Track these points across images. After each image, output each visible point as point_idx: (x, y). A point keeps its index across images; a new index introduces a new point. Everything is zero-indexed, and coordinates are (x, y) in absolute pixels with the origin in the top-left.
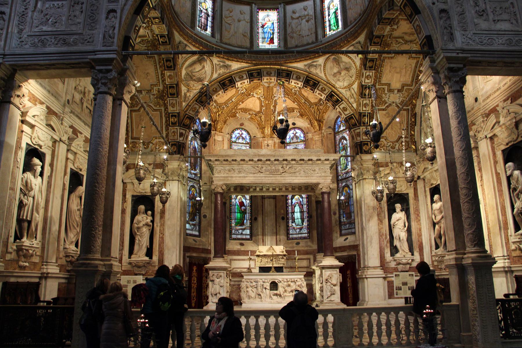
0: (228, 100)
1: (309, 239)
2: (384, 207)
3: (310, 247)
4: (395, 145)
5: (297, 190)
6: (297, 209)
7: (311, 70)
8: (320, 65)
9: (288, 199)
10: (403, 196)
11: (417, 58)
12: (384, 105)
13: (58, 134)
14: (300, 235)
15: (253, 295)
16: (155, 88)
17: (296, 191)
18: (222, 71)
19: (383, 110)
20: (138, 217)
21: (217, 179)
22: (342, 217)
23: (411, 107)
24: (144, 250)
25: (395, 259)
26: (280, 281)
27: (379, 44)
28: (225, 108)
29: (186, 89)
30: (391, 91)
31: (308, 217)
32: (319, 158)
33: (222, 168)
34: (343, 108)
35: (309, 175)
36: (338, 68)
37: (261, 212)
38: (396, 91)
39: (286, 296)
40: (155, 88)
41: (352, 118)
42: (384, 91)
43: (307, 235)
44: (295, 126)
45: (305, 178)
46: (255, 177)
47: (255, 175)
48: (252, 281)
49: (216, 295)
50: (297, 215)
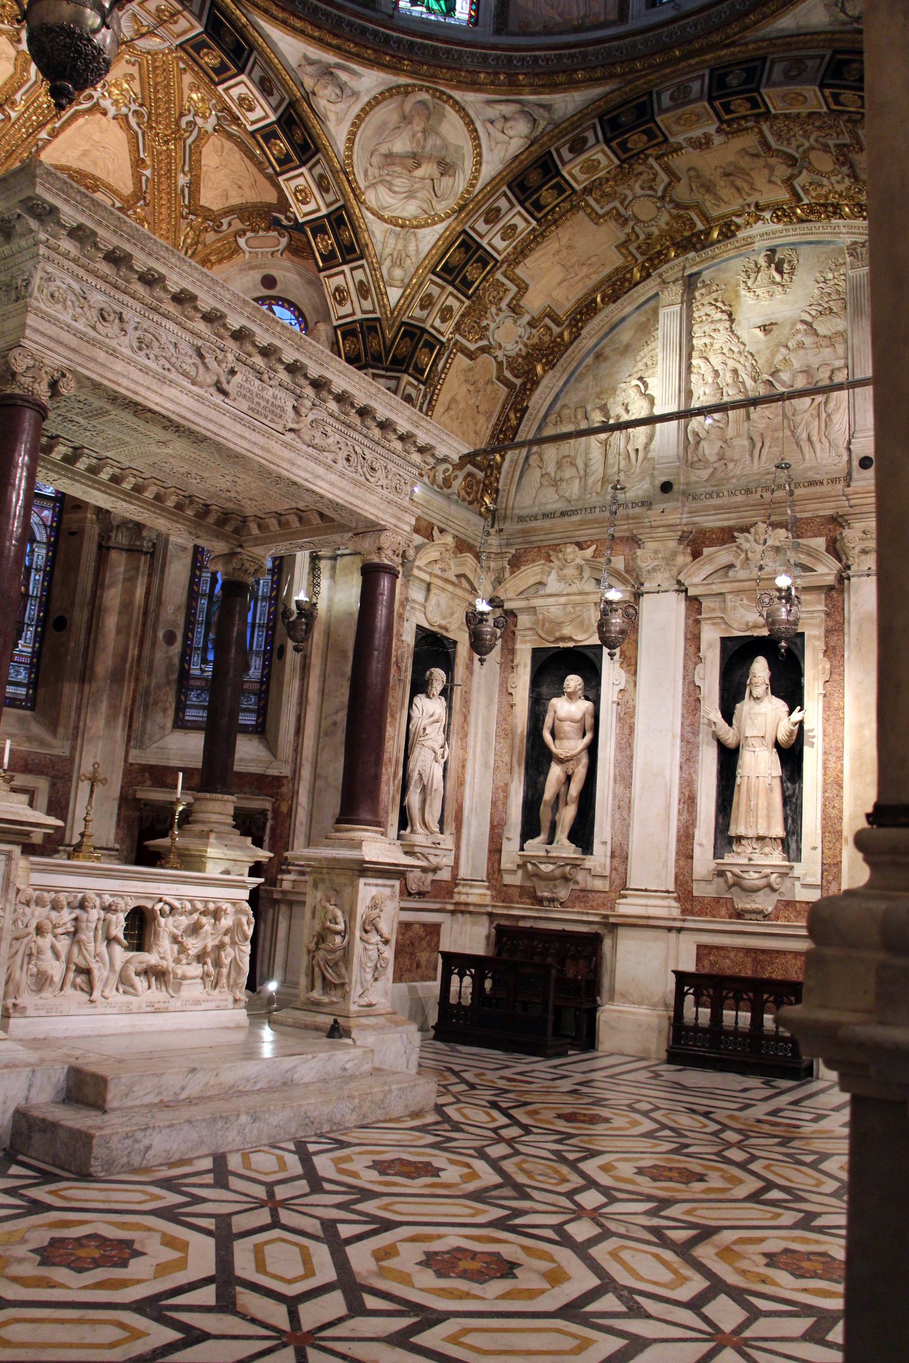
1: (32, 709)
2: (406, 671)
3: (42, 743)
4: (456, 477)
5: (190, 513)
7: (321, 92)
8: (355, 94)
10: (445, 647)
11: (634, 256)
12: (476, 342)
15: (56, 969)
17: (185, 519)
19: (471, 355)
21: (45, 327)
22: (196, 658)
23: (524, 384)
25: (417, 849)
26: (172, 908)
27: (624, 156)
30: (515, 309)
31: (42, 622)
32: (416, 431)
33: (76, 286)
34: (361, 282)
35: (357, 477)
36: (418, 142)
38: (527, 318)
39: (184, 978)
41: (374, 329)
42: (501, 299)
43: (22, 691)
45: (349, 487)
46: (199, 398)
47: (195, 389)
48: (63, 897)
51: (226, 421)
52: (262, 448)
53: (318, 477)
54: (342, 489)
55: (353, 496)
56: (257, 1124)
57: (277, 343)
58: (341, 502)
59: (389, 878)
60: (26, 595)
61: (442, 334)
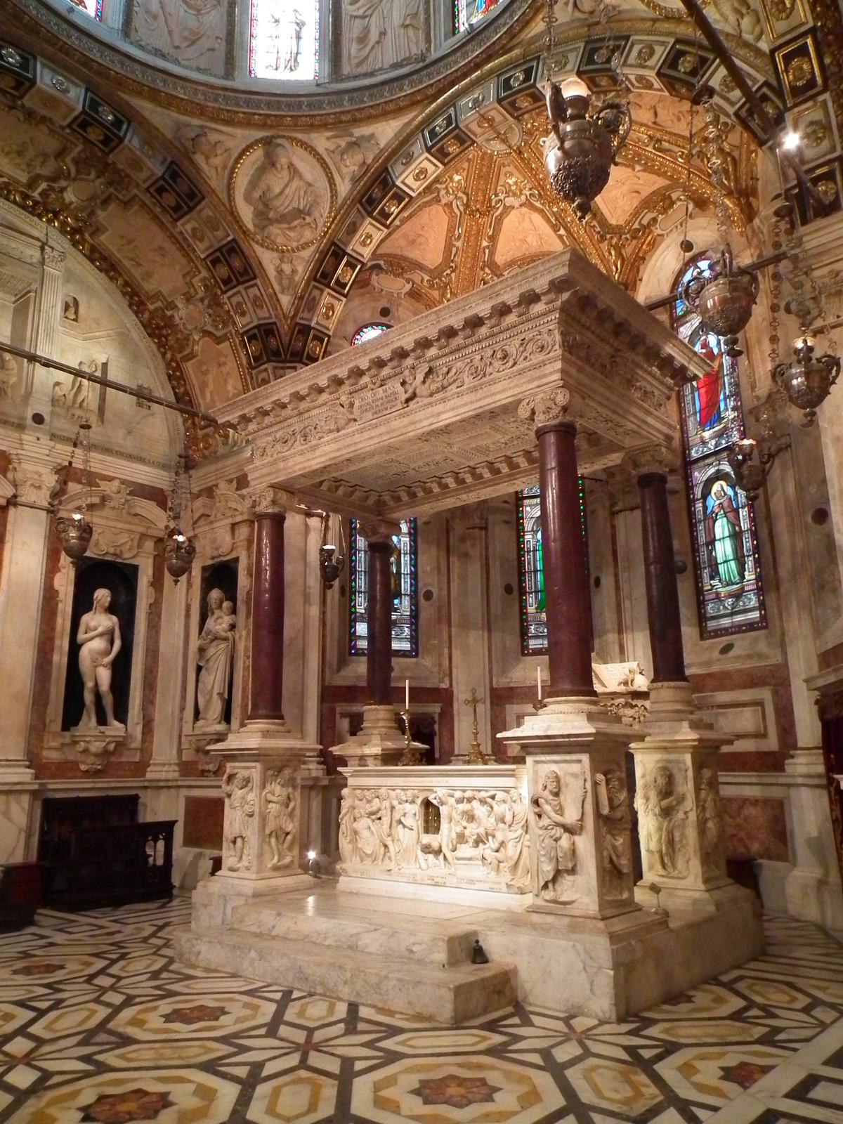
0: (449, 246)
6: (721, 528)
9: (694, 500)
14: (738, 618)
16: (195, 281)
18: (351, 165)
20: (210, 623)
21: (256, 474)
24: (217, 707)
28: (453, 275)
29: (275, 254)
32: (499, 300)
33: (270, 438)
37: (610, 559)
40: (195, 281)
44: (695, 251)
45: (473, 397)
49: (234, 842)
50: (724, 549)
51: (357, 438)
52: (388, 433)
53: (439, 414)
54: (465, 405)
55: (481, 399)
56: (262, 962)
57: (351, 365)
58: (474, 413)
59: (570, 753)
60: (741, 532)
61: (802, 24)
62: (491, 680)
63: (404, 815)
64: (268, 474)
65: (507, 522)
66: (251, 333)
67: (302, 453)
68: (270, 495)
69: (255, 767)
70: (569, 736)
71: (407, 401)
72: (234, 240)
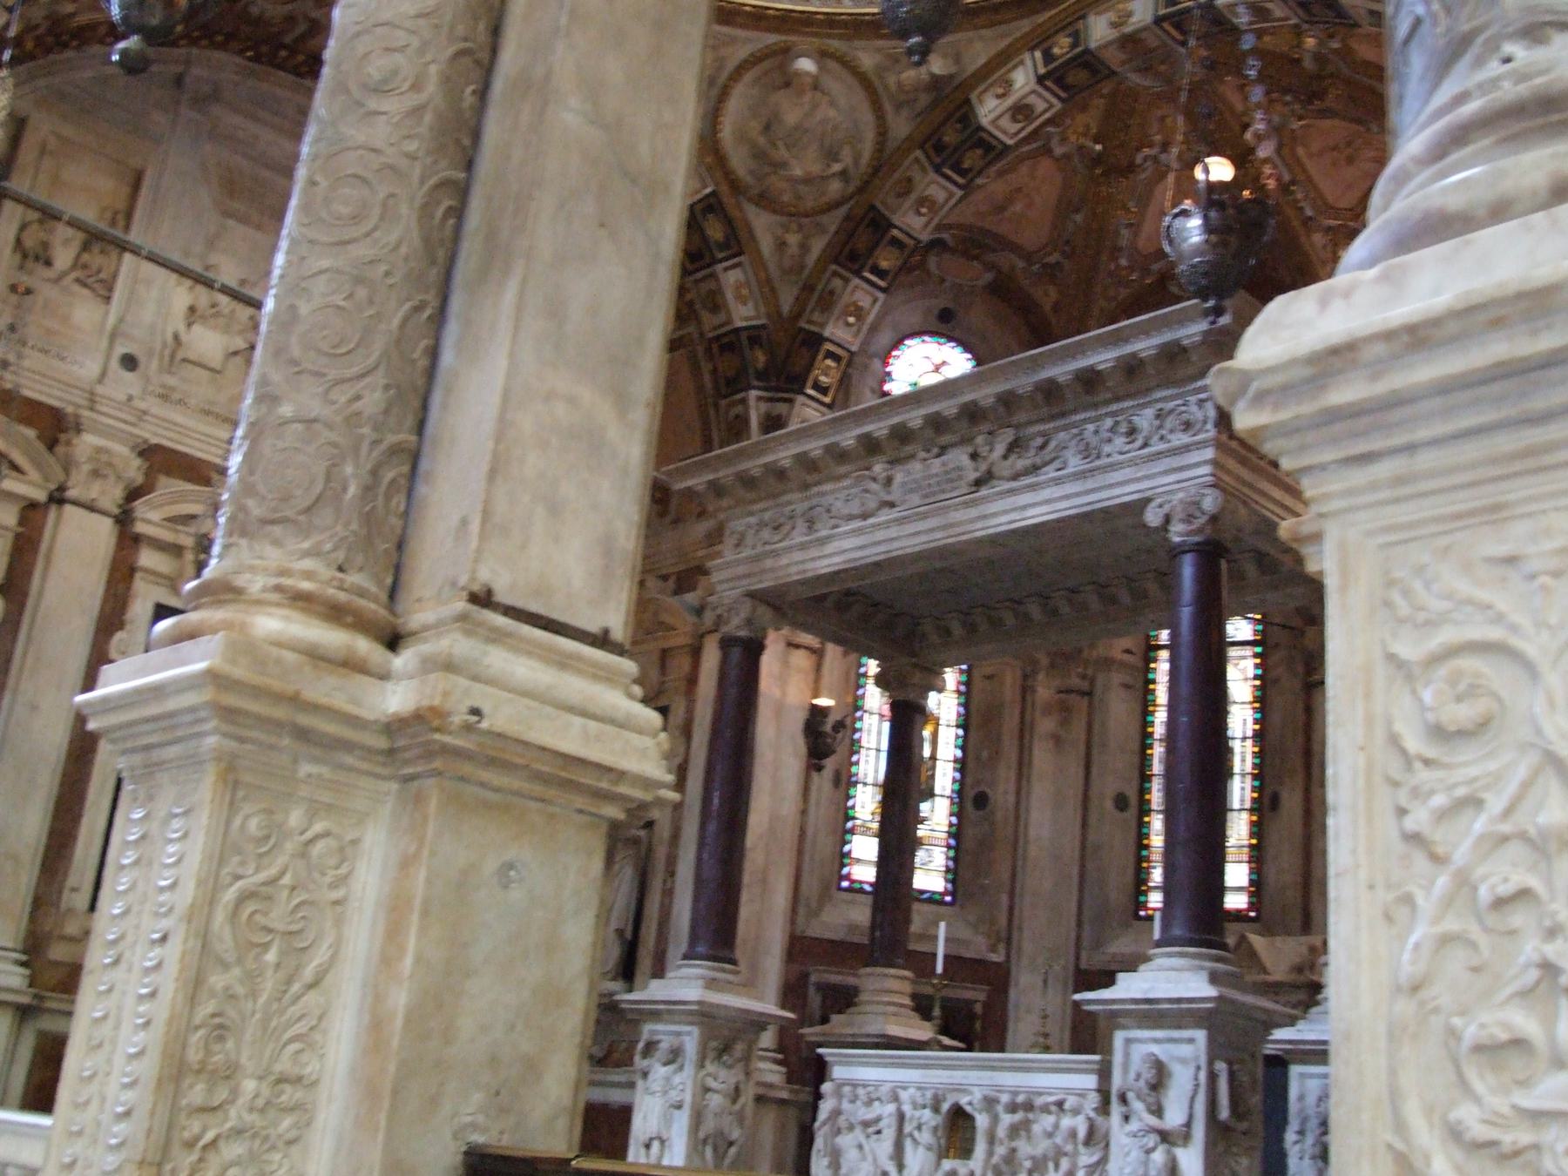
13: (34, 475)
32: (1128, 349)
33: (752, 520)
37: (1298, 762)
47: (871, 521)
49: (648, 1146)
51: (893, 532)
53: (1024, 508)
54: (1067, 497)
59: (1179, 1027)
62: (1078, 958)
63: (919, 1128)
64: (749, 576)
65: (1127, 686)
66: (725, 340)
67: (803, 547)
68: (745, 610)
69: (689, 1033)
70: (1179, 1000)
71: (978, 483)
72: (713, 194)
